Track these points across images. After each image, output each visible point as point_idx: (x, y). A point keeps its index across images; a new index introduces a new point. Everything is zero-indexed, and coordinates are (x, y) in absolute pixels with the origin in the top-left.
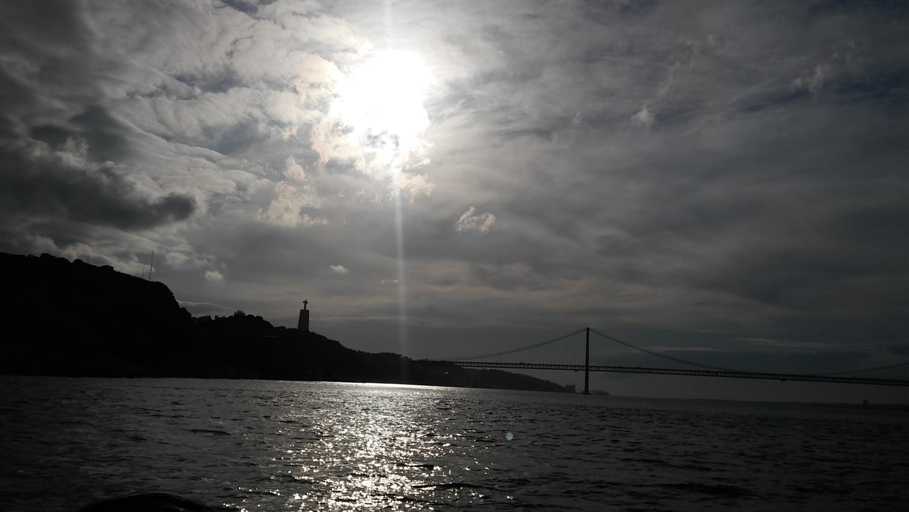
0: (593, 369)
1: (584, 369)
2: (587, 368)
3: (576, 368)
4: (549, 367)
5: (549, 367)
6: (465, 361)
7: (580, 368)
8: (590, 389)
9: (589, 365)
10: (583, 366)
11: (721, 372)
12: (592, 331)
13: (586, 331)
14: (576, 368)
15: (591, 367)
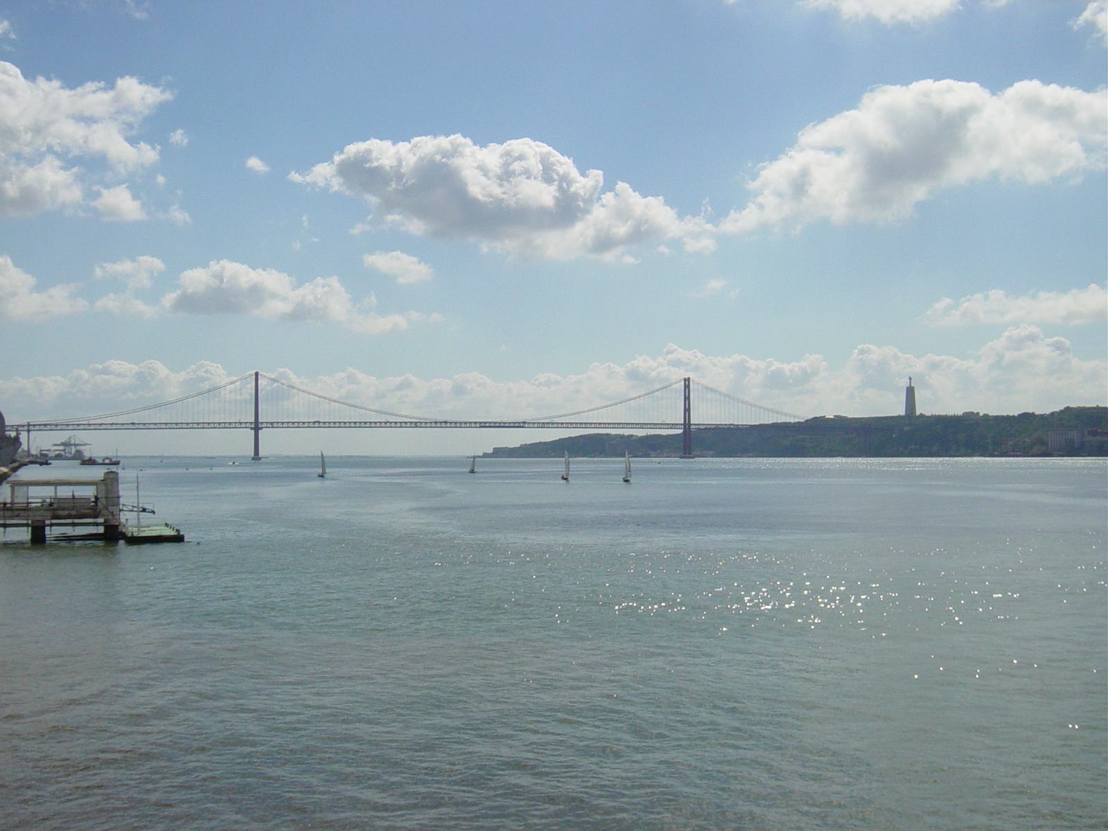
0: (265, 425)
1: (253, 426)
2: (257, 427)
3: (240, 425)
4: (206, 425)
5: (206, 425)
6: (80, 423)
7: (248, 425)
8: (261, 454)
9: (260, 421)
10: (251, 423)
11: (421, 423)
12: (261, 375)
13: (254, 377)
14: (240, 425)
15: (262, 423)
